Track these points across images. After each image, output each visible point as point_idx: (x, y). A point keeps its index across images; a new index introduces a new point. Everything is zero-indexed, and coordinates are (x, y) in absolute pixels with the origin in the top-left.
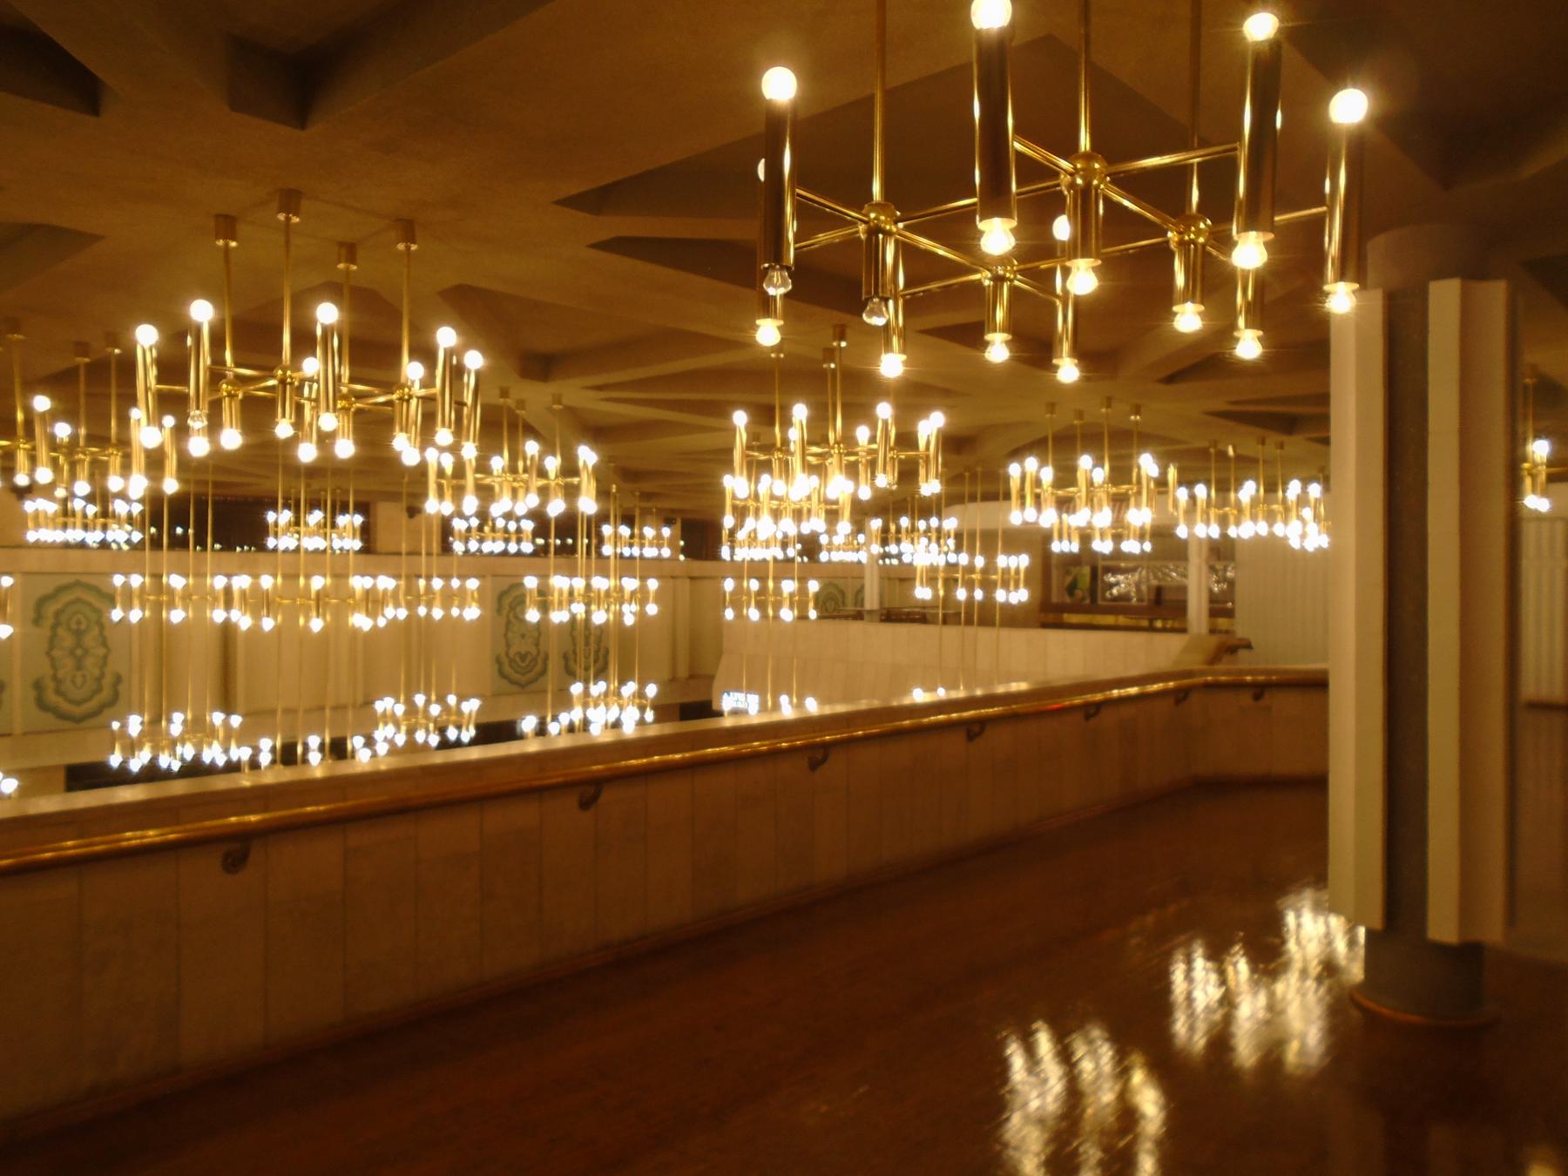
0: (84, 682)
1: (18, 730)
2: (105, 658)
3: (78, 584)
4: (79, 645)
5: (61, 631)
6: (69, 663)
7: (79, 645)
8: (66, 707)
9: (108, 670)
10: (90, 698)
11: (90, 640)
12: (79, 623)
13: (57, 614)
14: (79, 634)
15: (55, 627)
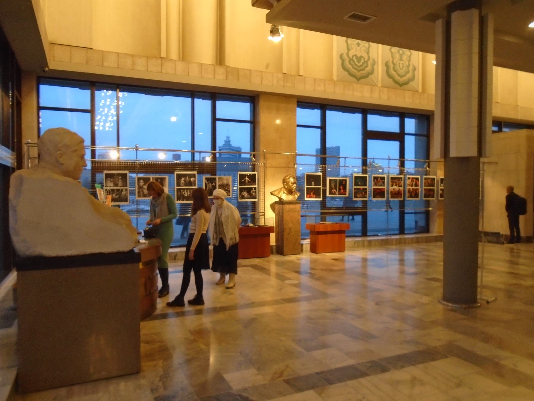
8: (397, 78)
9: (411, 63)
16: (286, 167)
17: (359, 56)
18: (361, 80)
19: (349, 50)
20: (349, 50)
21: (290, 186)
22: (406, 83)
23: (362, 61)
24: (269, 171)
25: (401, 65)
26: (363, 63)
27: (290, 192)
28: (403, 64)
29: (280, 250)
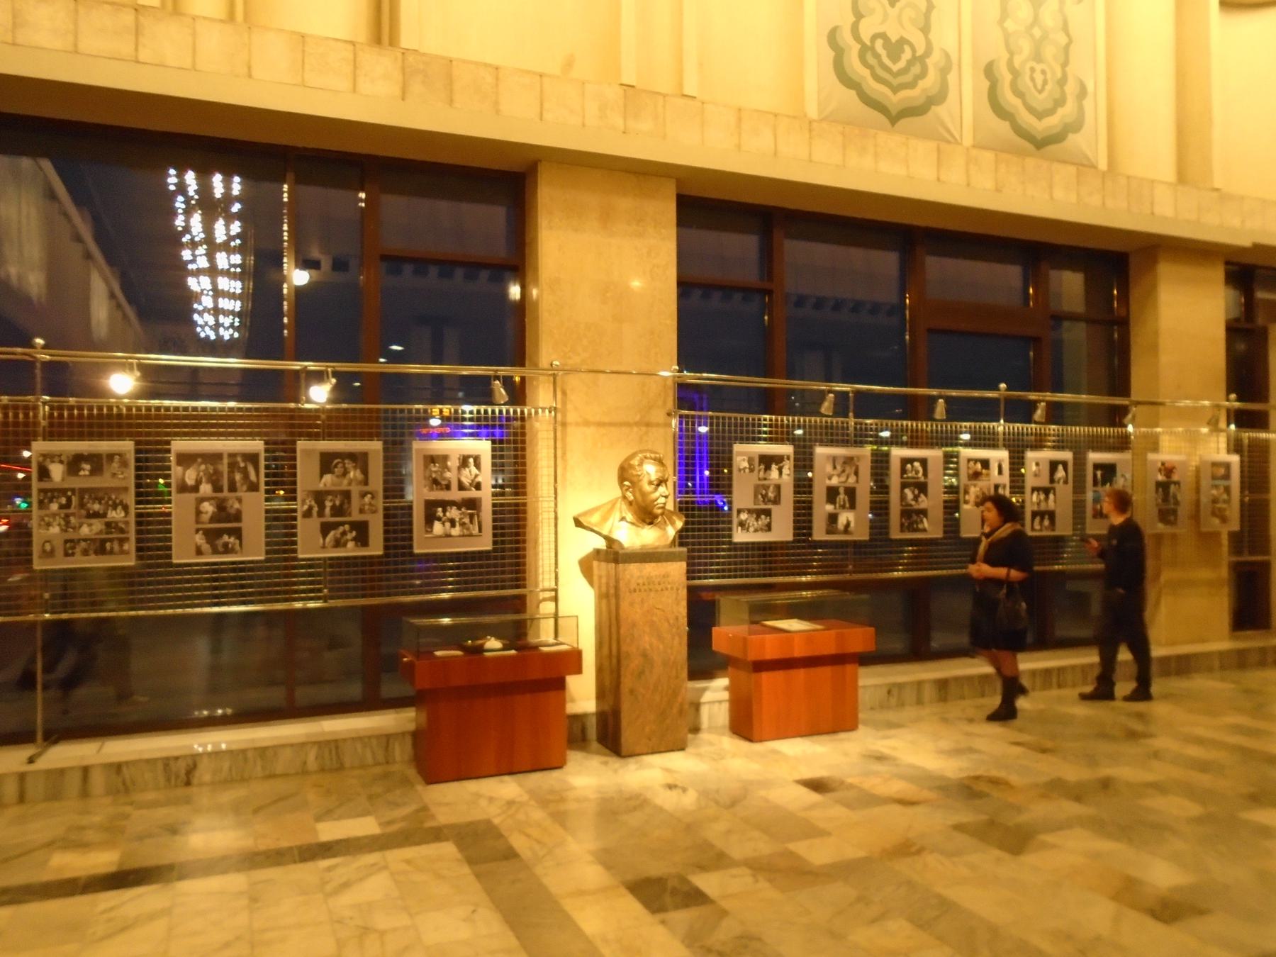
0: (1045, 82)
2: (1067, 49)
4: (1036, 21)
7: (1036, 21)
8: (1026, 119)
16: (637, 424)
19: (859, 16)
20: (859, 16)
21: (644, 494)
22: (1056, 138)
23: (907, 54)
24: (577, 438)
25: (1039, 79)
26: (910, 63)
27: (646, 515)
29: (609, 735)
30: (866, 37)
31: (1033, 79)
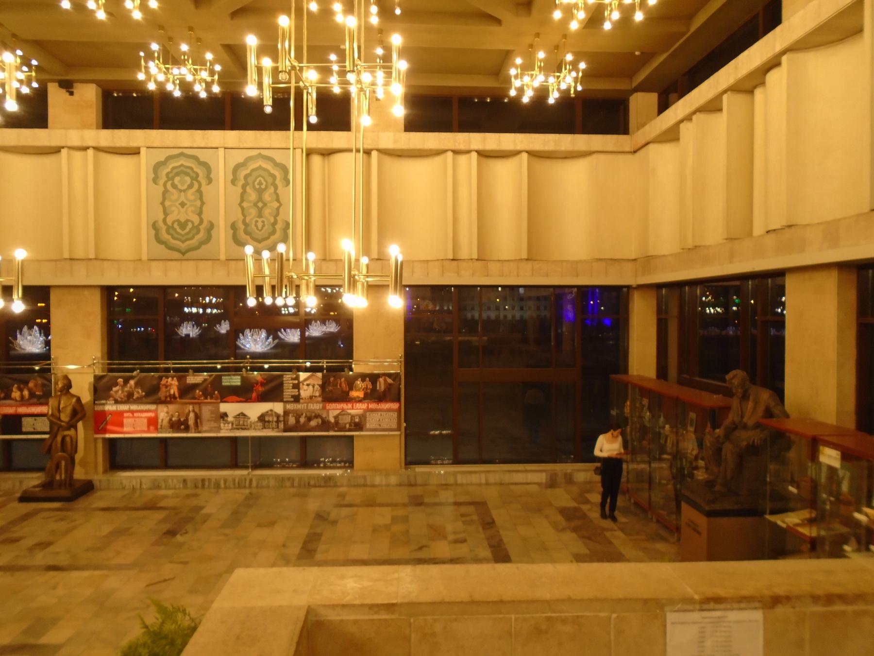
0: (263, 226)
1: (223, 257)
2: (278, 209)
3: (261, 156)
4: (260, 199)
5: (248, 189)
6: (254, 211)
7: (260, 199)
9: (279, 219)
10: (267, 238)
11: (267, 197)
12: (260, 183)
13: (246, 177)
14: (260, 192)
15: (244, 187)
17: (183, 220)
18: (188, 255)
23: (190, 225)
25: (260, 225)
28: (263, 222)
30: (170, 223)
31: (256, 226)
